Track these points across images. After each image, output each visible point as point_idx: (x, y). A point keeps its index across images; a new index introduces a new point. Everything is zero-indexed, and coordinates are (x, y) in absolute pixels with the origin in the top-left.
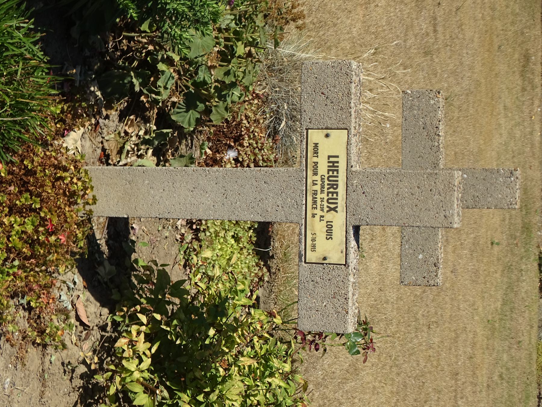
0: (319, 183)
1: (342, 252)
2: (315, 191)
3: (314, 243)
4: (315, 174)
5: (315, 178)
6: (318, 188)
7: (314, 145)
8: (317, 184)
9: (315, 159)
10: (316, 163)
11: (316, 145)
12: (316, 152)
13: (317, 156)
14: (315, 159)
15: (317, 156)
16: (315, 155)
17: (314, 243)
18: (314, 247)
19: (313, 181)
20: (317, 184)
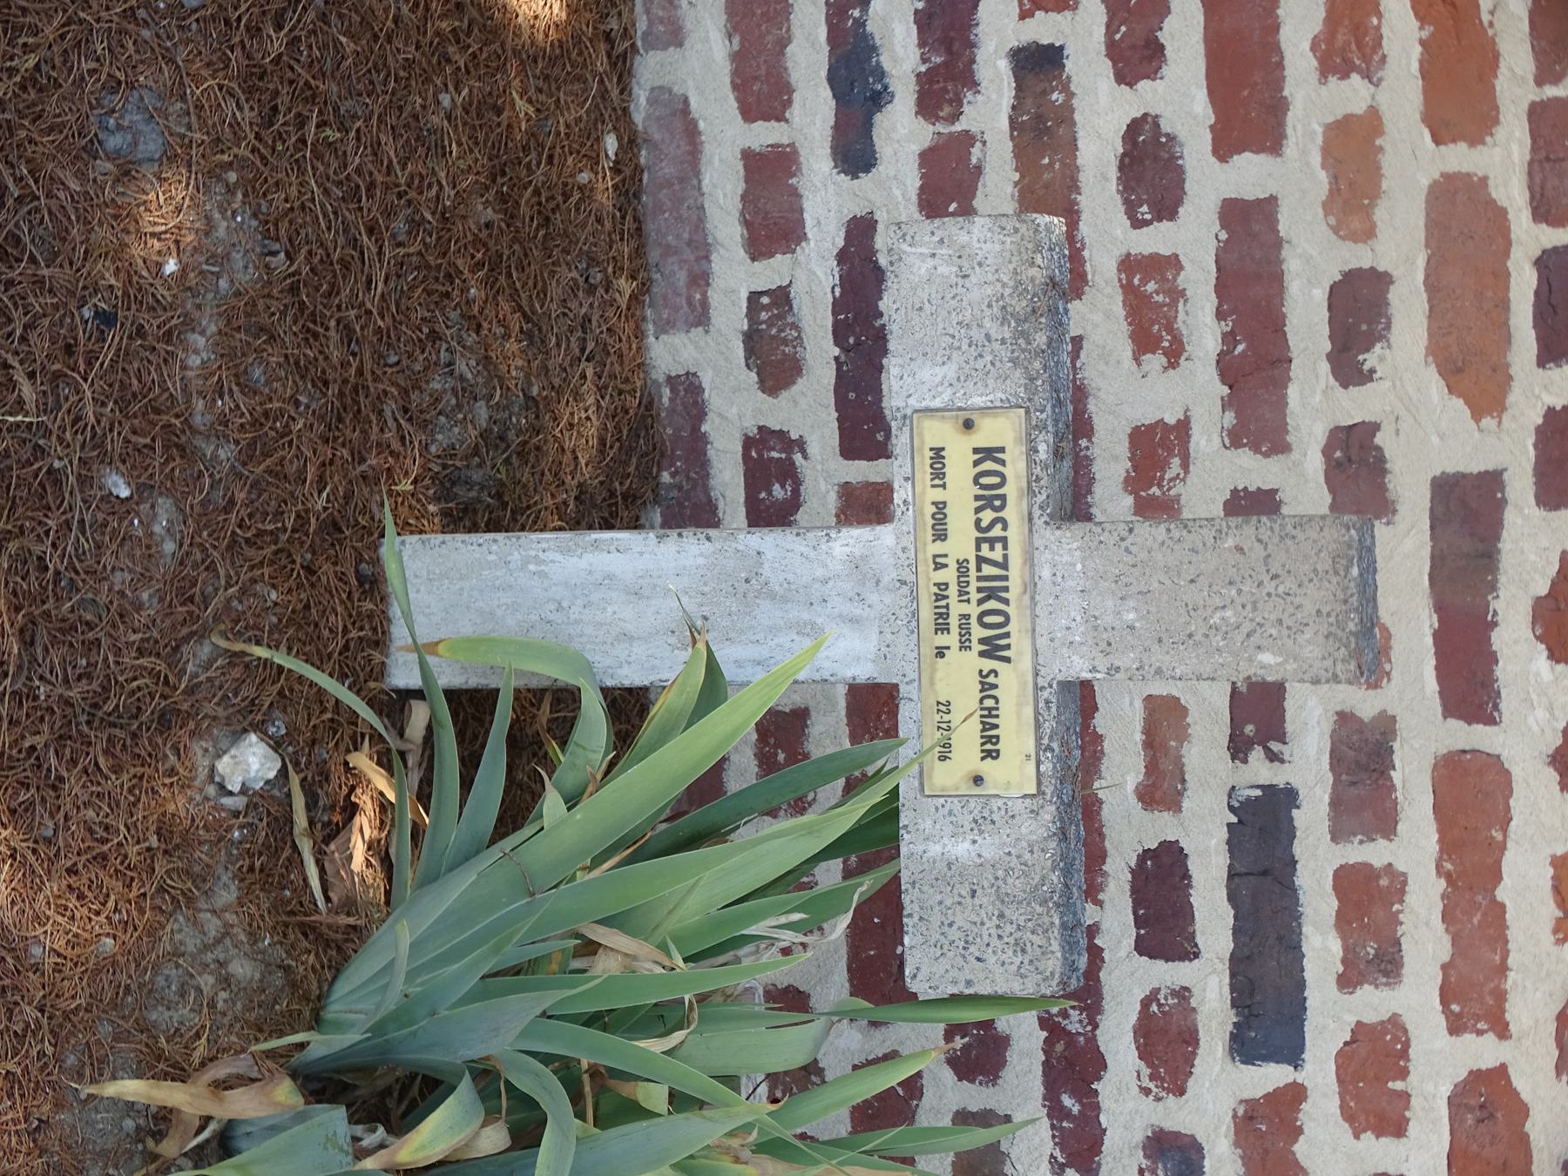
0: (953, 566)
1: (1028, 757)
2: (937, 585)
4: (941, 536)
5: (939, 547)
6: (949, 575)
7: (931, 454)
9: (938, 494)
10: (940, 506)
11: (938, 453)
12: (939, 474)
13: (944, 486)
14: (938, 494)
15: (944, 486)
16: (937, 482)
19: (935, 556)
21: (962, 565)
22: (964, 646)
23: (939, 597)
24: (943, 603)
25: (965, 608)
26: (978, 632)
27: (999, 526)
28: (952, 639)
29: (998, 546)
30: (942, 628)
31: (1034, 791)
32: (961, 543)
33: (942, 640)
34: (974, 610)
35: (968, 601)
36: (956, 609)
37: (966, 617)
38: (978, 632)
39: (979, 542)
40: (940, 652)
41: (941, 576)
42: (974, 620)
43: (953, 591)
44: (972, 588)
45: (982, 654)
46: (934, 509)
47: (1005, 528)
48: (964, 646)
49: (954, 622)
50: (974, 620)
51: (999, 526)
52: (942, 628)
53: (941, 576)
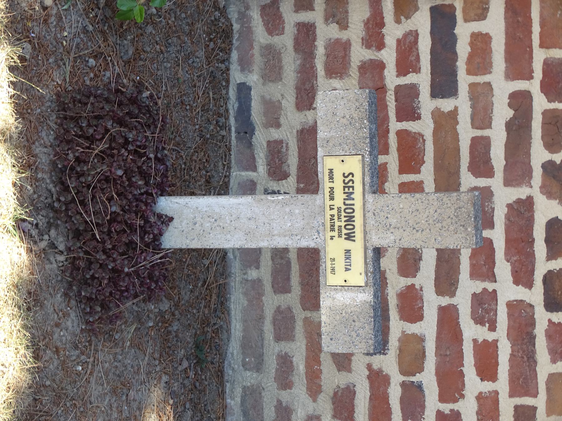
1: (361, 274)
2: (331, 215)
3: (333, 266)
4: (332, 199)
5: (332, 202)
6: (335, 212)
8: (333, 209)
9: (331, 185)
10: (332, 189)
11: (331, 171)
12: (331, 178)
13: (333, 182)
14: (331, 185)
15: (333, 182)
16: (331, 180)
17: (333, 266)
18: (333, 270)
19: (330, 206)
20: (333, 209)
21: (339, 209)
22: (340, 236)
23: (331, 219)
24: (333, 221)
25: (340, 224)
26: (344, 231)
27: (351, 182)
28: (336, 234)
29: (351, 189)
30: (332, 230)
31: (363, 284)
32: (339, 200)
33: (332, 234)
34: (343, 224)
35: (341, 221)
36: (337, 224)
37: (340, 226)
38: (344, 231)
39: (344, 187)
40: (332, 238)
41: (333, 212)
42: (343, 228)
43: (336, 218)
44: (342, 217)
45: (345, 239)
46: (330, 190)
47: (353, 190)
48: (340, 236)
49: (336, 228)
50: (343, 228)
51: (351, 182)
52: (332, 230)
53: (333, 212)
